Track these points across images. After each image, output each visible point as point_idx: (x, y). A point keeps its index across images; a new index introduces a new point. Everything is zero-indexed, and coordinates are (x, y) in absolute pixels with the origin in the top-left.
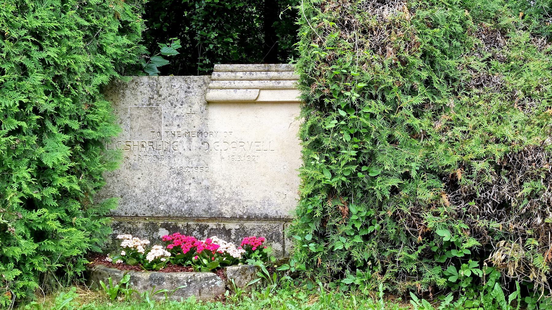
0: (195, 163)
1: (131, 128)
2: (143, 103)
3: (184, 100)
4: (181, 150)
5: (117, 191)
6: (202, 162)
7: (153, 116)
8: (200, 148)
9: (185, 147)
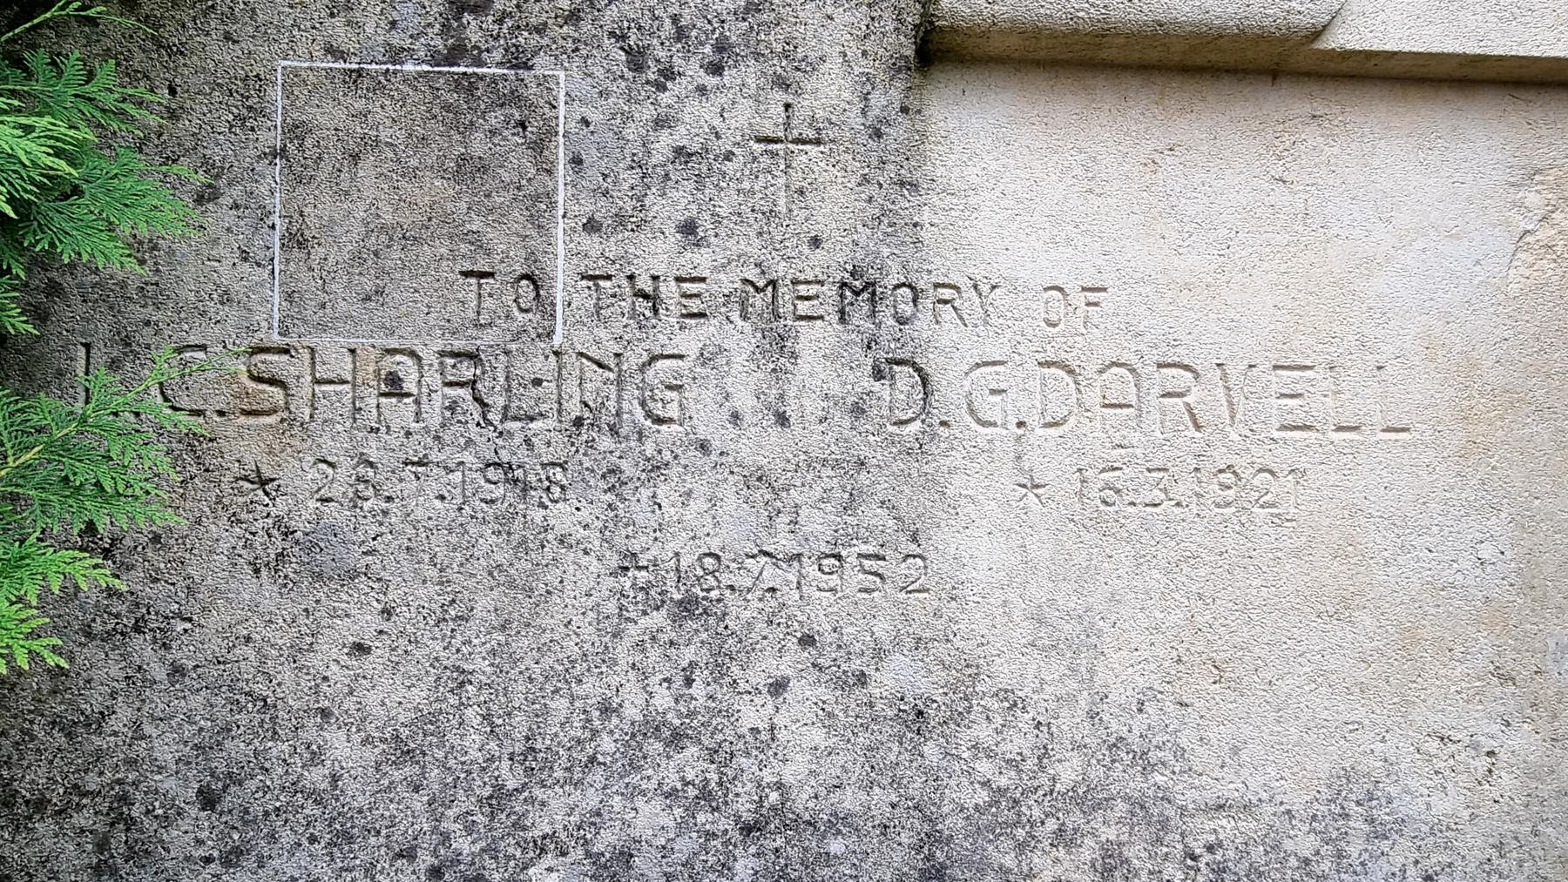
0: (819, 525)
1: (297, 241)
2: (397, 39)
3: (734, 31)
4: (707, 421)
5: (166, 753)
6: (873, 515)
7: (479, 145)
8: (858, 411)
9: (744, 401)
